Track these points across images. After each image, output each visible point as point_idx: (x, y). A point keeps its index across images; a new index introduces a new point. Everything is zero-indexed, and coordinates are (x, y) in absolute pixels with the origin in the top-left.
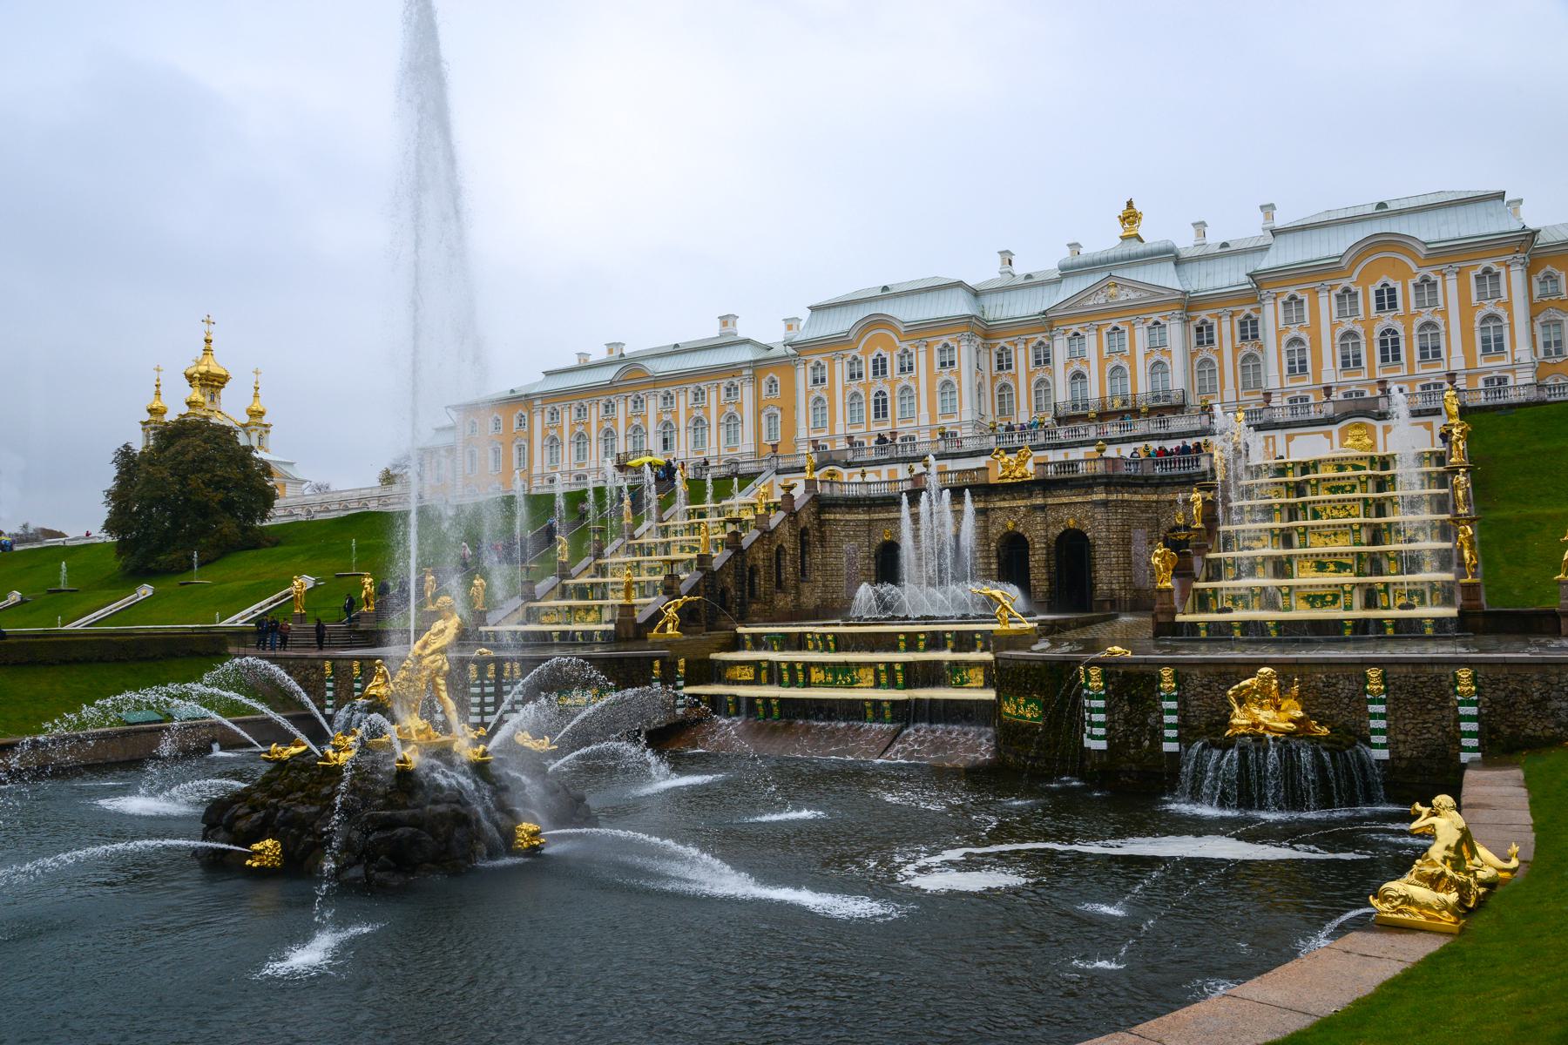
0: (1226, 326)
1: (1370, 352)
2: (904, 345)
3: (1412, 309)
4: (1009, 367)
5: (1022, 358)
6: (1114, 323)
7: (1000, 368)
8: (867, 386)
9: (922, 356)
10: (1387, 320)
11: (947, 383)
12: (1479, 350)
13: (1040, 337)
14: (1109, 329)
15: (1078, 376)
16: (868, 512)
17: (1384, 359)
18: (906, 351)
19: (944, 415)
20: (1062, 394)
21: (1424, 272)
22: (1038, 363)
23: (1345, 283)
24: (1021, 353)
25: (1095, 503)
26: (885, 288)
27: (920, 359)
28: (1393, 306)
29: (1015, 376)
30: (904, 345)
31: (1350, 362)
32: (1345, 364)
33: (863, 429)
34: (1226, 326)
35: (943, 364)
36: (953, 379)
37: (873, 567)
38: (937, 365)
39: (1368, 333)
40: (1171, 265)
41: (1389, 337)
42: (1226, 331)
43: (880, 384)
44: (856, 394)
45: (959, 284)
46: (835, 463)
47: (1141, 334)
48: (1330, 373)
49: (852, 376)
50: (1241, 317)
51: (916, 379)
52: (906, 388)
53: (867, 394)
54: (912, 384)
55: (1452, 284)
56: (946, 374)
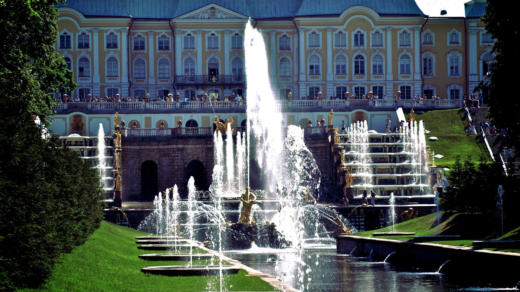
1: (350, 67)
2: (84, 30)
3: (371, 47)
4: (143, 48)
6: (213, 31)
7: (136, 48)
11: (112, 59)
12: (399, 72)
14: (209, 34)
15: (189, 61)
16: (138, 145)
17: (357, 72)
18: (84, 34)
21: (378, 28)
22: (160, 48)
23: (340, 28)
24: (151, 40)
27: (95, 41)
28: (362, 43)
30: (84, 30)
31: (341, 70)
32: (338, 72)
35: (109, 46)
36: (116, 56)
37: (140, 173)
38: (105, 46)
41: (359, 60)
47: (228, 39)
50: (281, 36)
52: (84, 59)
54: (88, 57)
56: (112, 52)
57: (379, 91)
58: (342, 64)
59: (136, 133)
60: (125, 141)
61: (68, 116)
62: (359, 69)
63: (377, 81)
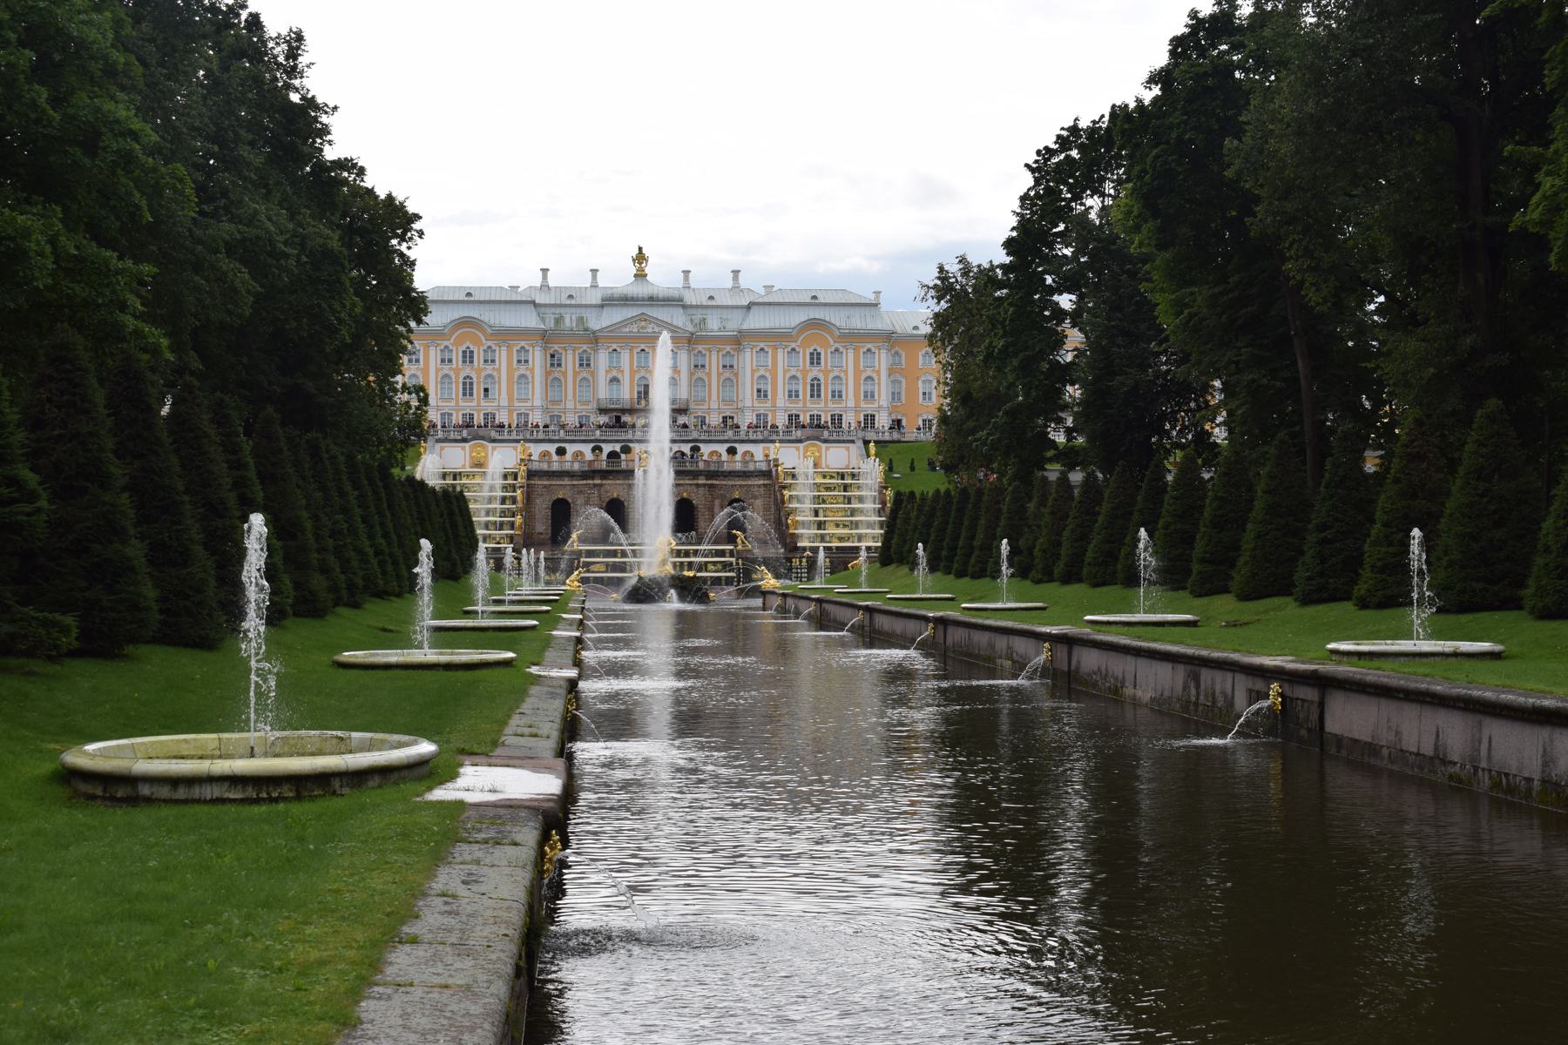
0: (714, 357)
1: (804, 390)
5: (570, 360)
8: (457, 371)
9: (504, 353)
10: (815, 372)
11: (523, 376)
13: (585, 347)
15: (614, 380)
19: (520, 400)
20: (603, 392)
23: (793, 345)
24: (570, 357)
25: (698, 486)
26: (469, 294)
27: (502, 356)
29: (564, 374)
33: (453, 404)
34: (714, 357)
39: (804, 379)
40: (681, 310)
42: (714, 361)
43: (467, 371)
44: (446, 376)
45: (533, 302)
46: (483, 438)
48: (782, 400)
49: (443, 361)
51: (499, 370)
53: (457, 376)
55: (851, 352)
56: (522, 370)
57: (837, 420)
58: (794, 388)
59: (545, 467)
60: (531, 474)
61: (467, 445)
62: (815, 390)
63: (835, 407)
